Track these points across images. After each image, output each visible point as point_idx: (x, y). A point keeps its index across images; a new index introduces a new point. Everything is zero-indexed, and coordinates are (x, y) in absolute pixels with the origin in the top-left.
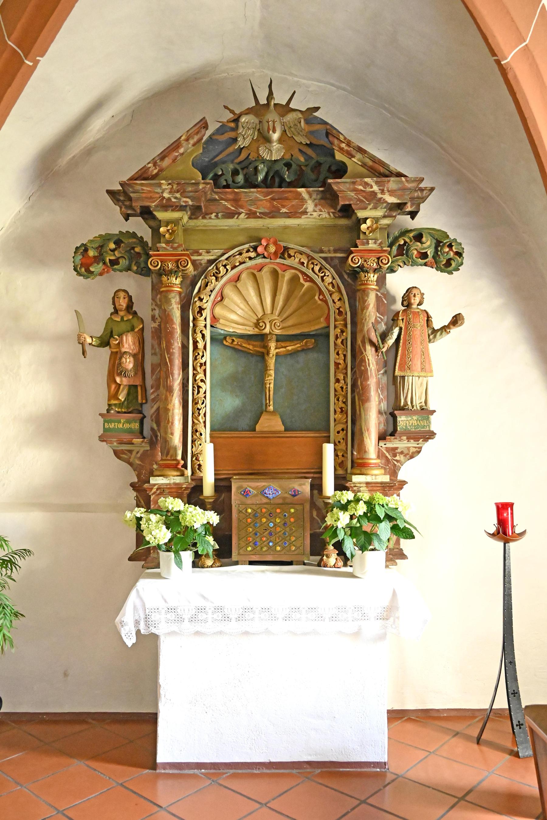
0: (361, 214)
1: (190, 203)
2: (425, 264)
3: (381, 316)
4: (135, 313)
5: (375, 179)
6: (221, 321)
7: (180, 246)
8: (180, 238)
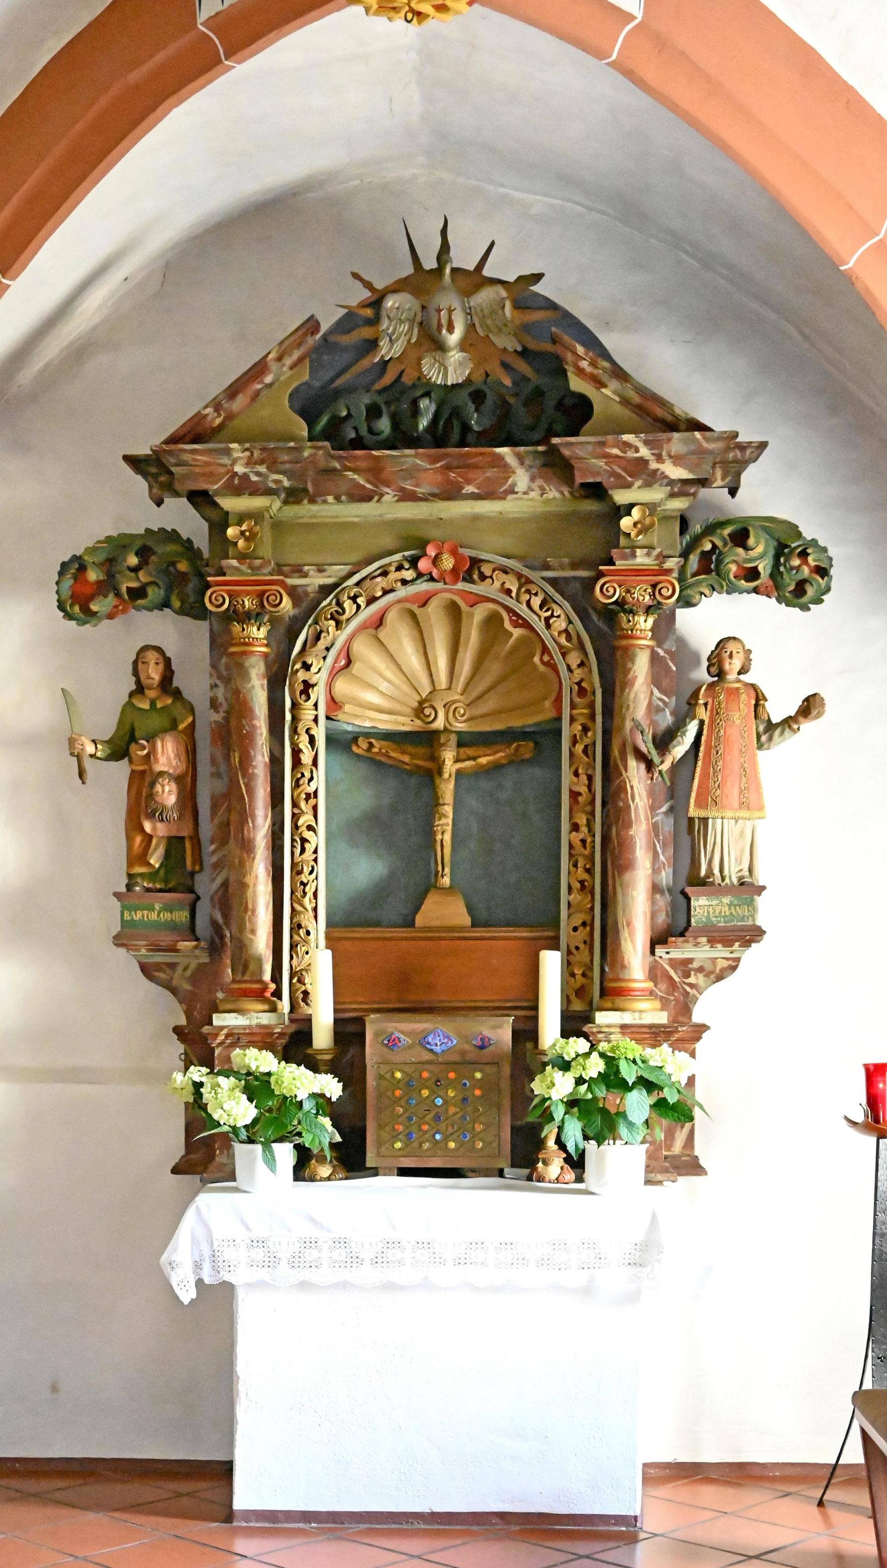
4: (177, 694)
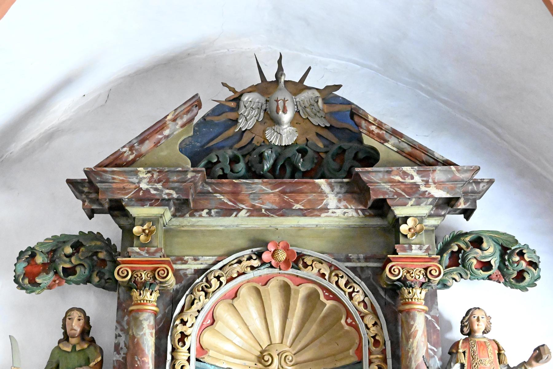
0: (399, 212)
1: (175, 196)
2: (489, 278)
3: (433, 348)
4: (92, 341)
5: (416, 167)
6: (211, 353)
7: (159, 250)
8: (159, 241)
